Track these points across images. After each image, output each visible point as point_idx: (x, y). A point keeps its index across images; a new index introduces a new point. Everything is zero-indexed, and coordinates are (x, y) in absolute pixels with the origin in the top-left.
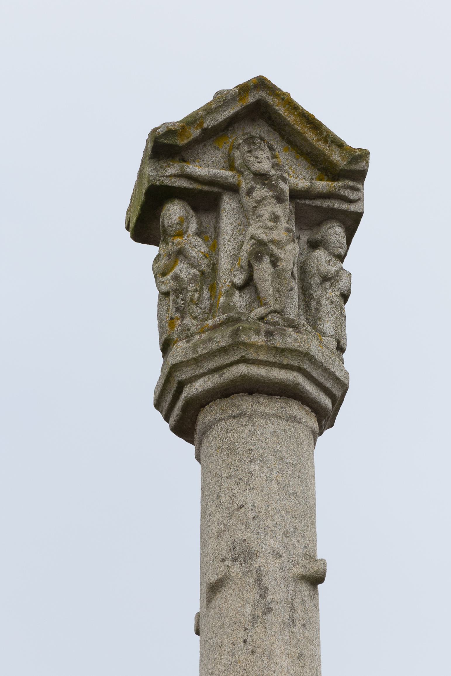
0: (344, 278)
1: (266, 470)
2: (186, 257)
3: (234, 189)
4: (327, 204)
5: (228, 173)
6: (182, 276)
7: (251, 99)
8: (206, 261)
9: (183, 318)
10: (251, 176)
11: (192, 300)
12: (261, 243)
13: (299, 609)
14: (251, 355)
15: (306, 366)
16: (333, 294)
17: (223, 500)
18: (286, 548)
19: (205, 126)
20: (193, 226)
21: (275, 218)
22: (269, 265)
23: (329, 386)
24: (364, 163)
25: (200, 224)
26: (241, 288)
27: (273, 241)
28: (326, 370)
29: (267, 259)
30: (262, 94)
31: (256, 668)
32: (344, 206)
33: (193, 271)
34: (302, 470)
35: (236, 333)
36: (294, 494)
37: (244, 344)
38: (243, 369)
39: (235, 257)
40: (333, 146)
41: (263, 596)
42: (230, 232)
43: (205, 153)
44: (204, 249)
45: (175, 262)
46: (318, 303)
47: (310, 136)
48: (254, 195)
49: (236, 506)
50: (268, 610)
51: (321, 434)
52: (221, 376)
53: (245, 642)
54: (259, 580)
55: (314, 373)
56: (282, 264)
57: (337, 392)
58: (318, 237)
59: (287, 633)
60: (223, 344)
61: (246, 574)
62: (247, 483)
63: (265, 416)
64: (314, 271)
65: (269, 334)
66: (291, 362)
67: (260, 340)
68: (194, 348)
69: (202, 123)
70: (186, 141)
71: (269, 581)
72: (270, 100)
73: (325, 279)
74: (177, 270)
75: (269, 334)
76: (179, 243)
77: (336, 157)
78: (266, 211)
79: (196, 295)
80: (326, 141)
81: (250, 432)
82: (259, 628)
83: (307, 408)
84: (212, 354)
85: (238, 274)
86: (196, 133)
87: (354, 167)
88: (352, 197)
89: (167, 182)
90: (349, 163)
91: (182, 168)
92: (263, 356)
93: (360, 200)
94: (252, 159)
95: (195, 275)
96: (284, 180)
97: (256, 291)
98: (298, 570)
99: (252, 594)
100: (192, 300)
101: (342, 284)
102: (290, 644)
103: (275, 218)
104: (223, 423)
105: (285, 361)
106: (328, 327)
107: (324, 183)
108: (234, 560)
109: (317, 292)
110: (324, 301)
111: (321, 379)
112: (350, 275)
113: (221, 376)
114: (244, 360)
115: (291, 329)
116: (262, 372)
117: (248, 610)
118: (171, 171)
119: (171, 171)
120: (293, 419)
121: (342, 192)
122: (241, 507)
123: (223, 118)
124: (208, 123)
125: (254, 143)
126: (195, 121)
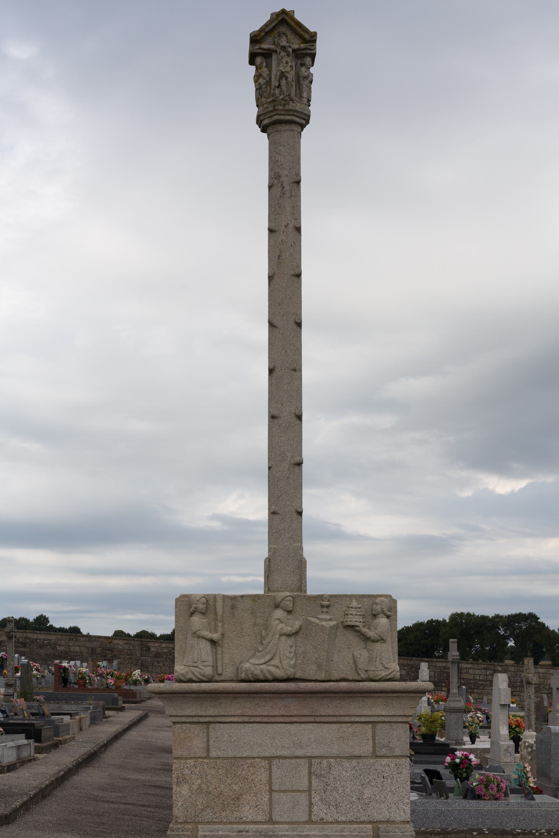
0: (311, 76)
1: (284, 148)
2: (262, 76)
3: (275, 51)
4: (305, 51)
5: (273, 47)
6: (261, 83)
7: (280, 18)
8: (268, 77)
9: (261, 98)
10: (280, 47)
11: (264, 91)
12: (282, 73)
13: (293, 193)
14: (279, 113)
15: (295, 114)
16: (307, 82)
17: (273, 159)
18: (290, 173)
19: (266, 31)
20: (265, 64)
21: (287, 63)
22: (285, 80)
23: (304, 117)
24: (315, 37)
25: (266, 63)
26: (277, 87)
27: (286, 72)
28: (302, 113)
29: (284, 78)
30: (284, 16)
31: (281, 212)
32: (310, 52)
33: (265, 81)
34: (295, 147)
35: (274, 106)
36: (292, 155)
37: (277, 109)
38: (277, 117)
39: (276, 76)
40: (306, 33)
41: (283, 189)
42: (275, 67)
43: (267, 39)
44: (268, 72)
45: (259, 78)
46: (302, 86)
47: (298, 29)
48: (281, 55)
49: (276, 161)
50: (284, 194)
51: (302, 130)
52: (271, 119)
53: (278, 204)
54: (282, 185)
55: (298, 115)
56: (289, 79)
57: (307, 118)
58: (303, 62)
59: (289, 200)
60: (271, 109)
61: (278, 183)
62: (279, 153)
63: (284, 131)
64: (301, 75)
65: (284, 105)
66: (291, 113)
67: (281, 108)
68: (264, 110)
69: (265, 30)
70: (260, 37)
71: (285, 185)
72: (286, 18)
73: (304, 78)
74: (259, 81)
75: (284, 105)
76: (260, 72)
77: (306, 36)
78: (284, 60)
79: (265, 89)
80: (303, 31)
81: (280, 136)
82: (282, 200)
83: (297, 125)
84: (268, 112)
85: (277, 82)
86: (263, 34)
87: (312, 39)
88: (312, 49)
89: (256, 51)
90: (311, 38)
91: (260, 46)
92: (282, 113)
93: (315, 49)
94: (280, 42)
95: (265, 82)
96: (290, 47)
97: (281, 88)
98: (293, 180)
99: (280, 189)
100: (264, 91)
101: (310, 78)
102: (290, 203)
103: (287, 63)
104: (273, 133)
105: (289, 113)
106: (305, 95)
107: (303, 45)
108: (275, 178)
109: (302, 82)
110: (304, 86)
111: (301, 116)
112: (312, 74)
113: (271, 119)
114: (277, 114)
115: (291, 102)
116: (282, 117)
117: (279, 194)
118: (257, 47)
119: (257, 47)
120: (293, 130)
121: (309, 47)
122: (277, 161)
123: (272, 27)
124: (267, 30)
125: (281, 36)
126: (262, 30)
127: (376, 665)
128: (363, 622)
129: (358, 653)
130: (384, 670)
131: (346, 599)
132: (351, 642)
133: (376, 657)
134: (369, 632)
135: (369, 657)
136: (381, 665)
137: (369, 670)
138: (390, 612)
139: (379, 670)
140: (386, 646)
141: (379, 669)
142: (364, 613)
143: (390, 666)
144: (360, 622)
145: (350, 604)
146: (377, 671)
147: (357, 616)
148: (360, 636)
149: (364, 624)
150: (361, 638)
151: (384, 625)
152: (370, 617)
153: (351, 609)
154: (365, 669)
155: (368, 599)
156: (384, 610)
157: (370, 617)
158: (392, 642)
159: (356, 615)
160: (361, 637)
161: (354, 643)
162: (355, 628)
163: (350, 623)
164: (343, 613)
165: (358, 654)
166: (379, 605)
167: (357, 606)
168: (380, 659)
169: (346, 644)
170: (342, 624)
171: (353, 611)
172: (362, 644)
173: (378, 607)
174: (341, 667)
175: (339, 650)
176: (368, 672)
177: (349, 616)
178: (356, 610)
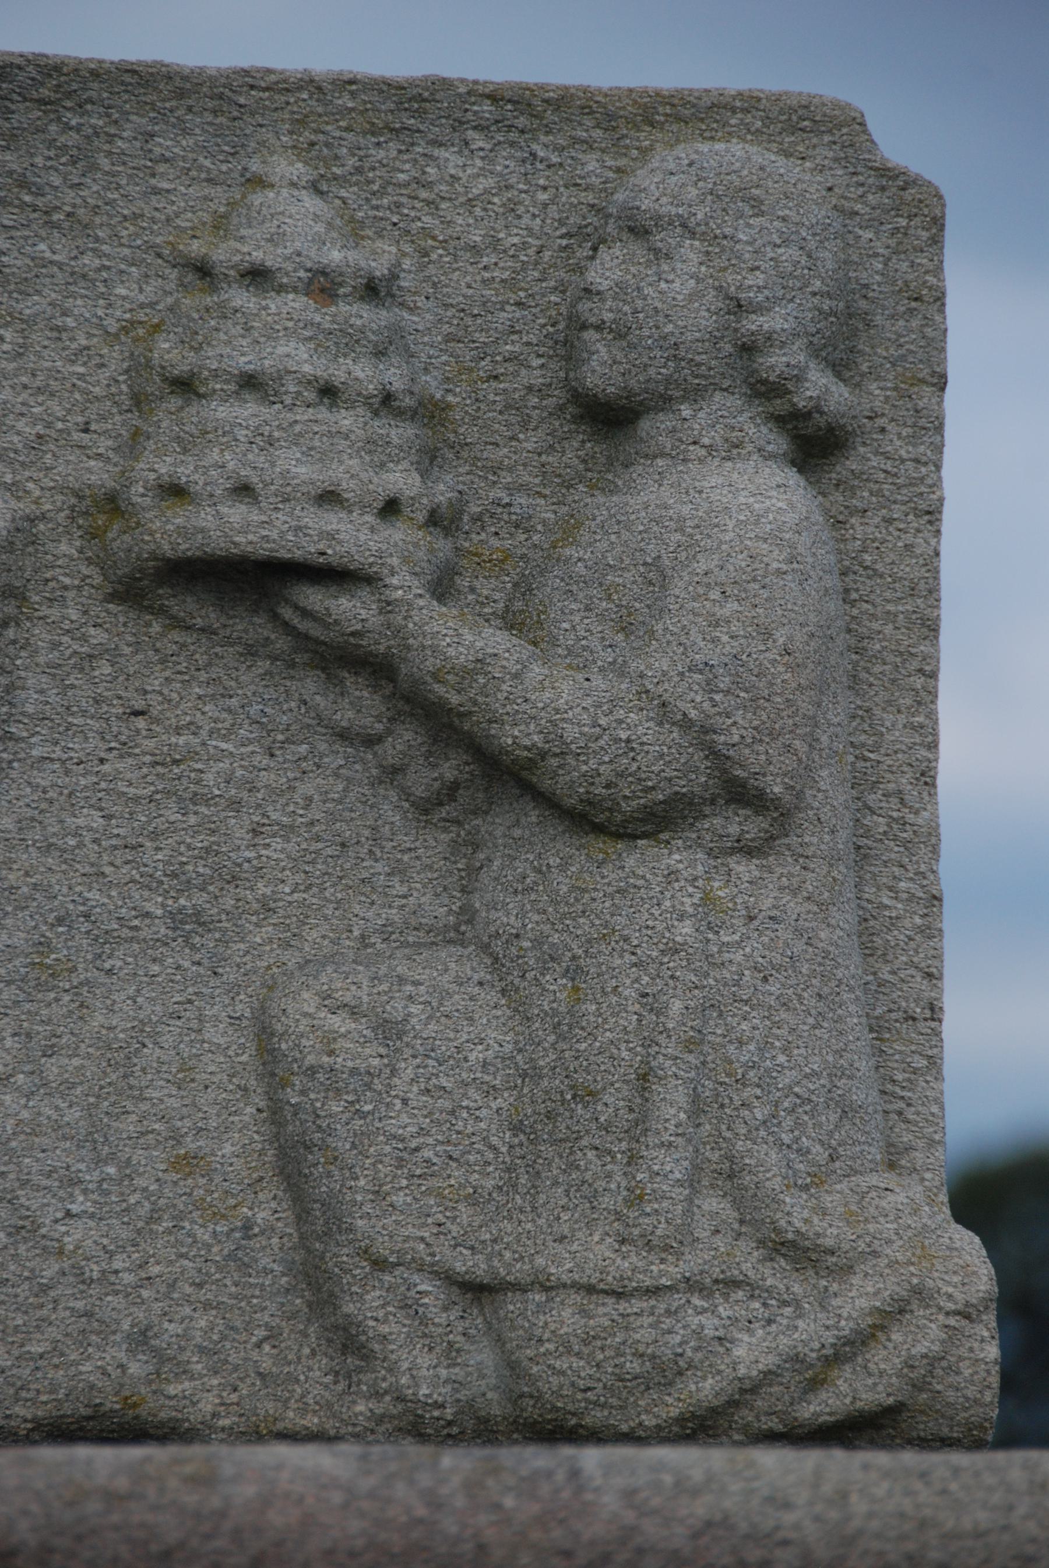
127: (636, 1198)
128: (434, 520)
129: (354, 1012)
130: (753, 1289)
131: (162, 145)
132: (238, 828)
133: (645, 1077)
134: (537, 670)
135: (530, 1074)
136: (712, 1203)
137: (520, 1271)
138: (840, 368)
139: (691, 1285)
140: (794, 907)
141: (690, 1264)
142: (432, 384)
143: (850, 1219)
144: (391, 508)
145: (220, 225)
146: (654, 1291)
147: (346, 420)
148: (371, 741)
149: (444, 546)
150: (393, 773)
151: (776, 559)
152: (530, 442)
153: (241, 298)
154: (463, 1263)
155: (506, 162)
156: (752, 323)
157: (530, 442)
158: (862, 855)
159: (329, 392)
160: (392, 750)
161: (276, 848)
162: (313, 597)
163: (236, 513)
164: (115, 358)
165: (338, 1022)
166: (690, 252)
167: (335, 256)
168: (697, 1109)
169: (155, 857)
170: (93, 534)
171: (271, 334)
172: (399, 871)
173: (680, 287)
174: (74, 1235)
175: (44, 945)
176: (512, 1304)
177: (222, 411)
178: (324, 317)
